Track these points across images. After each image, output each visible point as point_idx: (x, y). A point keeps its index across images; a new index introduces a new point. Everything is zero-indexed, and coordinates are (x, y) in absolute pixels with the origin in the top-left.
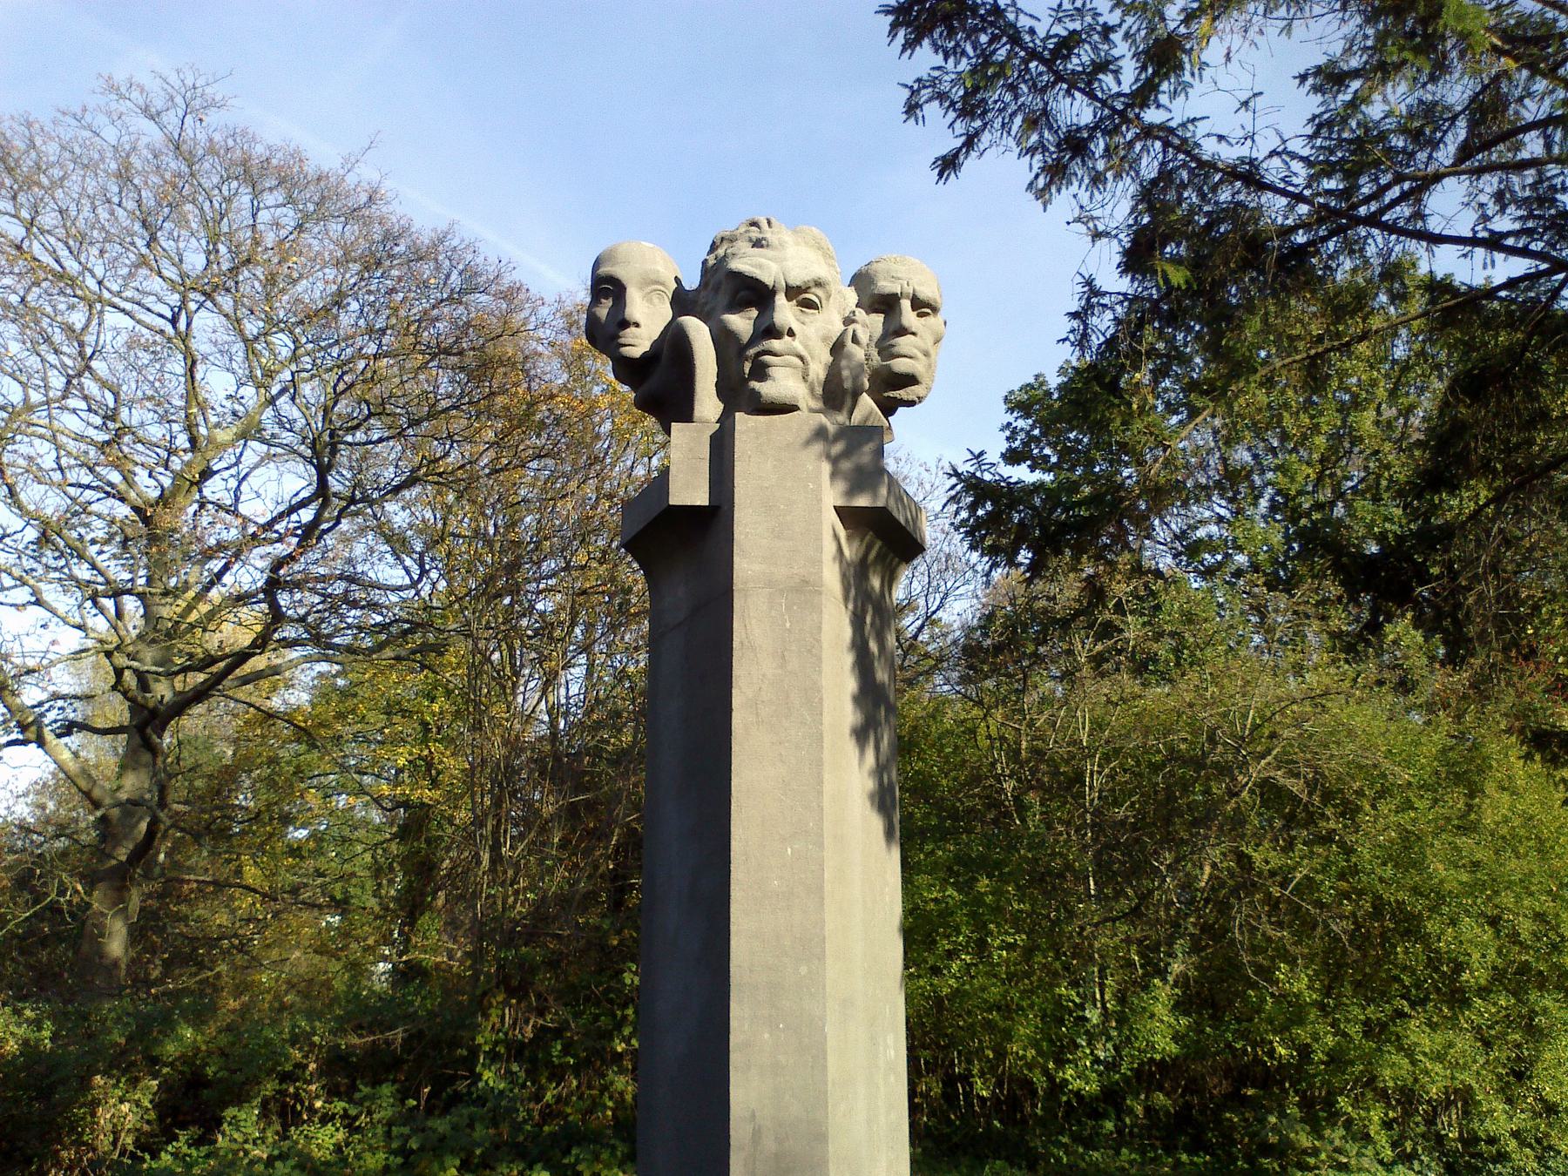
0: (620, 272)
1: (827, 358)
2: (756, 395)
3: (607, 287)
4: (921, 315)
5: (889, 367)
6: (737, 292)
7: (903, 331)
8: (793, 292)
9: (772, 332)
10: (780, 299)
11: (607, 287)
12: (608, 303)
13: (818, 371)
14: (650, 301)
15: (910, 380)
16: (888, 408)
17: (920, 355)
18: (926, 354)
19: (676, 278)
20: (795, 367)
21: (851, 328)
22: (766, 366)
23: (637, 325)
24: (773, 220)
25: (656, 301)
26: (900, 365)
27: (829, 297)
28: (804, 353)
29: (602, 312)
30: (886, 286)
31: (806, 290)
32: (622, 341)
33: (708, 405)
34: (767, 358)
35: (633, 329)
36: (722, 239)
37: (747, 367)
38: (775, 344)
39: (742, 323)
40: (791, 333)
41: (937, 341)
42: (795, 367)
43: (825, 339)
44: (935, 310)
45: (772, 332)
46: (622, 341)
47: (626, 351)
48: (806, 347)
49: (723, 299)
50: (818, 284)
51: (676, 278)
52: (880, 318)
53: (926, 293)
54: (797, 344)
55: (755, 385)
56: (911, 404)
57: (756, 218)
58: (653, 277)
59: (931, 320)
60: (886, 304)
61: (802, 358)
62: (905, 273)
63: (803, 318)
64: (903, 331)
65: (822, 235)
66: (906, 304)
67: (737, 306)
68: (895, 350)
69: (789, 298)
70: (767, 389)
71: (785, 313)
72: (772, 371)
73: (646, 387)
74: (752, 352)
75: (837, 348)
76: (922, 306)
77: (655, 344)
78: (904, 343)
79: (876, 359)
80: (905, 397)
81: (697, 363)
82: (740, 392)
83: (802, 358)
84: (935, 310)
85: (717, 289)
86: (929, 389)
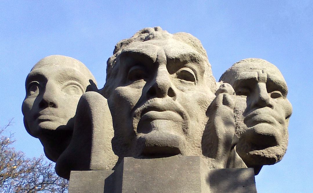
0: (44, 70)
1: (203, 119)
2: (143, 141)
3: (36, 82)
4: (274, 96)
5: (254, 131)
6: (128, 68)
7: (263, 103)
8: (175, 65)
9: (154, 91)
10: (163, 69)
11: (36, 82)
12: (35, 94)
13: (198, 125)
14: (67, 92)
15: (270, 140)
16: (257, 164)
17: (277, 122)
18: (281, 122)
19: (91, 81)
20: (176, 121)
21: (221, 96)
22: (152, 119)
23: (54, 105)
24: (159, 28)
25: (72, 92)
26: (262, 128)
27: (203, 72)
28: (182, 109)
29: (32, 101)
30: (245, 74)
31: (184, 63)
32: (41, 117)
33: (104, 156)
34: (152, 113)
35: (49, 109)
36: (122, 44)
37: (136, 123)
38: (159, 101)
39: (133, 91)
40: (172, 93)
41: (288, 117)
42: (176, 121)
43: (201, 102)
44: (284, 92)
45: (154, 91)
46: (41, 117)
47: (45, 125)
48: (185, 106)
49: (120, 78)
50: (194, 59)
51: (91, 81)
52: (244, 98)
53: (278, 77)
54: (178, 103)
55: (141, 135)
56: (271, 161)
57: (146, 28)
58: (70, 74)
59: (281, 100)
60: (247, 87)
61: (181, 113)
62: (259, 66)
63: (182, 86)
64: (263, 103)
65: (194, 38)
66: (263, 86)
67: (129, 79)
68: (257, 118)
69: (171, 72)
70: (152, 136)
71: (164, 77)
72: (157, 123)
73: (62, 155)
74: (139, 109)
75: (211, 110)
76: (274, 87)
77: (71, 120)
78: (263, 112)
79: (243, 127)
80: (267, 155)
81: (95, 123)
82: (126, 144)
83: (181, 113)
84: (284, 92)
85: (115, 75)
86: (285, 150)
